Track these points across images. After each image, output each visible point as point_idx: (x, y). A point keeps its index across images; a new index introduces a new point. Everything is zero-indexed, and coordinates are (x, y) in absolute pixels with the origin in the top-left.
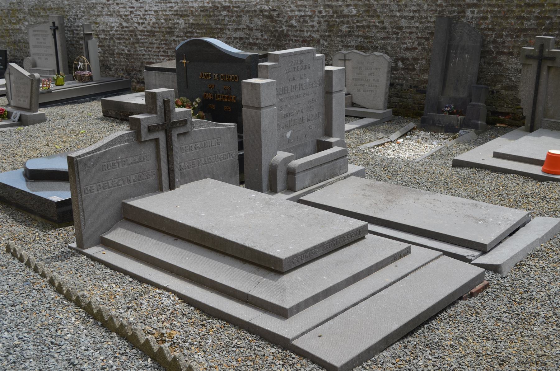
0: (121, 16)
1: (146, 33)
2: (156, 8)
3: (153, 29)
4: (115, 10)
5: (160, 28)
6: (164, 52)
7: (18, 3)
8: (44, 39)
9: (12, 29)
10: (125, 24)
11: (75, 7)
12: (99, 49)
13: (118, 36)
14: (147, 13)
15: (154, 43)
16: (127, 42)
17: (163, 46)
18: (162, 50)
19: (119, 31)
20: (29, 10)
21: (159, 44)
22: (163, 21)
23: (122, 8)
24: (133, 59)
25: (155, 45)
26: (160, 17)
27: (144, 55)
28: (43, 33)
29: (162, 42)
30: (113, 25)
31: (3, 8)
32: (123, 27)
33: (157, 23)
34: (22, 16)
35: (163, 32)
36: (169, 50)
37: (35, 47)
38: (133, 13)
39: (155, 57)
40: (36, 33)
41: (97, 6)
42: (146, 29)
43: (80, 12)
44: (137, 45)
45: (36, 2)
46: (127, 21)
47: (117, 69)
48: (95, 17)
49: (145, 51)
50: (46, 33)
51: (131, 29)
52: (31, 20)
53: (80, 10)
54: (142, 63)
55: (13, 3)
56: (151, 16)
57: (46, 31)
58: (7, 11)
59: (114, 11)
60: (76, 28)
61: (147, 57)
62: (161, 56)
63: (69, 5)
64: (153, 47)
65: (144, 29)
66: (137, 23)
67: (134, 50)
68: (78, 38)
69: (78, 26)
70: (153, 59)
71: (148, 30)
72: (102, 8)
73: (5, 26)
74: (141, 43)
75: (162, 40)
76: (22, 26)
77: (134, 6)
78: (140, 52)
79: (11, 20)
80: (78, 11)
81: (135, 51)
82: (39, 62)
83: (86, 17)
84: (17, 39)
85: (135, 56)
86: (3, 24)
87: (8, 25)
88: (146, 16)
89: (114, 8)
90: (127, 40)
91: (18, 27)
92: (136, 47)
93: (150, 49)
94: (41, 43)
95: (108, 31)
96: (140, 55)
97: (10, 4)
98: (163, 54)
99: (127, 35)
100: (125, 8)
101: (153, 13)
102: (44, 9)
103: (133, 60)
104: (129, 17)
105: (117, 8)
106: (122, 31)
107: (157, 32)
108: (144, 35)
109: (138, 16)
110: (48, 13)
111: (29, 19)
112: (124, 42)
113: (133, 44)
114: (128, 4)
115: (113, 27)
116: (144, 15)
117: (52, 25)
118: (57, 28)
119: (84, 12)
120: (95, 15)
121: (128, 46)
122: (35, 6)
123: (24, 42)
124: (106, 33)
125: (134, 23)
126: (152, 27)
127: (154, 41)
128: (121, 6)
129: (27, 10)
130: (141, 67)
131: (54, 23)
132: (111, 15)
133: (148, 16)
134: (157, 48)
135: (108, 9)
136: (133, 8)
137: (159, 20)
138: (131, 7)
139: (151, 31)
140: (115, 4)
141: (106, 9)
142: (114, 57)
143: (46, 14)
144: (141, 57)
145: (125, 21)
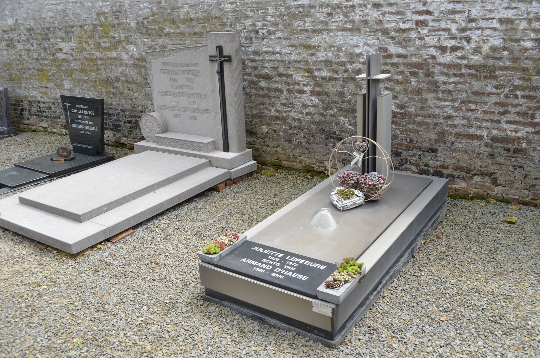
0: (385, 32)
1: (463, 71)
2: (510, 14)
3: (491, 62)
4: (368, 18)
5: (515, 60)
6: (518, 114)
7: (114, 12)
8: (189, 80)
9: (101, 59)
10: (394, 49)
11: (251, 14)
12: (313, 98)
14: (474, 25)
15: (489, 94)
16: (398, 88)
17: (521, 101)
18: (513, 110)
20: (138, 24)
21: (506, 96)
22: (528, 44)
23: (391, 13)
24: (414, 123)
25: (493, 99)
26: (519, 35)
27: (449, 117)
28: (186, 68)
29: (518, 93)
30: (358, 51)
31: (83, 23)
32: (390, 56)
33: (504, 49)
34: (123, 36)
35: (525, 70)
37: (165, 93)
38: (427, 25)
39: (488, 124)
40: (170, 68)
41: (312, 11)
42: (465, 62)
43: (264, 25)
44: (429, 96)
45: (154, 9)
46: (405, 42)
48: (306, 34)
49: (456, 109)
50: (194, 69)
51: (414, 60)
52: (142, 41)
53: (265, 20)
54: (442, 134)
55: (104, 13)
56: (487, 32)
57: (196, 65)
58: (91, 28)
59: (366, 22)
60: (252, 56)
61: (457, 122)
63: (235, 11)
64: (485, 103)
65: (459, 61)
67: (419, 105)
68: (256, 76)
69: (257, 53)
70: (480, 128)
71: (472, 62)
72: (329, 14)
73: (89, 54)
75: (516, 88)
76: (123, 54)
77: (431, 9)
78: (437, 112)
79: (99, 43)
80: (259, 24)
81: (422, 108)
82: (173, 122)
83: (278, 35)
84: (113, 76)
85: (420, 119)
86: (86, 50)
87: (93, 51)
88: (468, 33)
89: (366, 15)
90: (398, 82)
91: (114, 54)
92: (426, 100)
93: (473, 106)
94: (181, 87)
95: (344, 64)
96: (435, 117)
97: (98, 15)
98: (518, 119)
99: (402, 72)
100: (398, 13)
101: (495, 24)
102: (173, 22)
103: (410, 126)
104: (413, 35)
105: (376, 14)
106: (386, 64)
107: (506, 68)
108: (455, 75)
109: (441, 33)
110: (182, 28)
111: (138, 41)
113: (418, 92)
114: (412, 6)
115: (359, 55)
116: (464, 30)
117: (214, 52)
118: (229, 59)
119: (275, 24)
120: (307, 31)
121: (401, 97)
122: (152, 16)
123: (127, 81)
124: (334, 67)
125: (425, 46)
126: (488, 56)
127: (490, 89)
128: (385, 9)
129: (133, 25)
130: (437, 141)
131: (220, 49)
132: (355, 30)
133: (479, 32)
134: (496, 104)
135: (346, 16)
136: (428, 13)
137: (517, 41)
138: (421, 13)
139: (485, 66)
140: (369, 6)
141: (342, 17)
143: (177, 31)
144: (441, 120)
145: (399, 43)
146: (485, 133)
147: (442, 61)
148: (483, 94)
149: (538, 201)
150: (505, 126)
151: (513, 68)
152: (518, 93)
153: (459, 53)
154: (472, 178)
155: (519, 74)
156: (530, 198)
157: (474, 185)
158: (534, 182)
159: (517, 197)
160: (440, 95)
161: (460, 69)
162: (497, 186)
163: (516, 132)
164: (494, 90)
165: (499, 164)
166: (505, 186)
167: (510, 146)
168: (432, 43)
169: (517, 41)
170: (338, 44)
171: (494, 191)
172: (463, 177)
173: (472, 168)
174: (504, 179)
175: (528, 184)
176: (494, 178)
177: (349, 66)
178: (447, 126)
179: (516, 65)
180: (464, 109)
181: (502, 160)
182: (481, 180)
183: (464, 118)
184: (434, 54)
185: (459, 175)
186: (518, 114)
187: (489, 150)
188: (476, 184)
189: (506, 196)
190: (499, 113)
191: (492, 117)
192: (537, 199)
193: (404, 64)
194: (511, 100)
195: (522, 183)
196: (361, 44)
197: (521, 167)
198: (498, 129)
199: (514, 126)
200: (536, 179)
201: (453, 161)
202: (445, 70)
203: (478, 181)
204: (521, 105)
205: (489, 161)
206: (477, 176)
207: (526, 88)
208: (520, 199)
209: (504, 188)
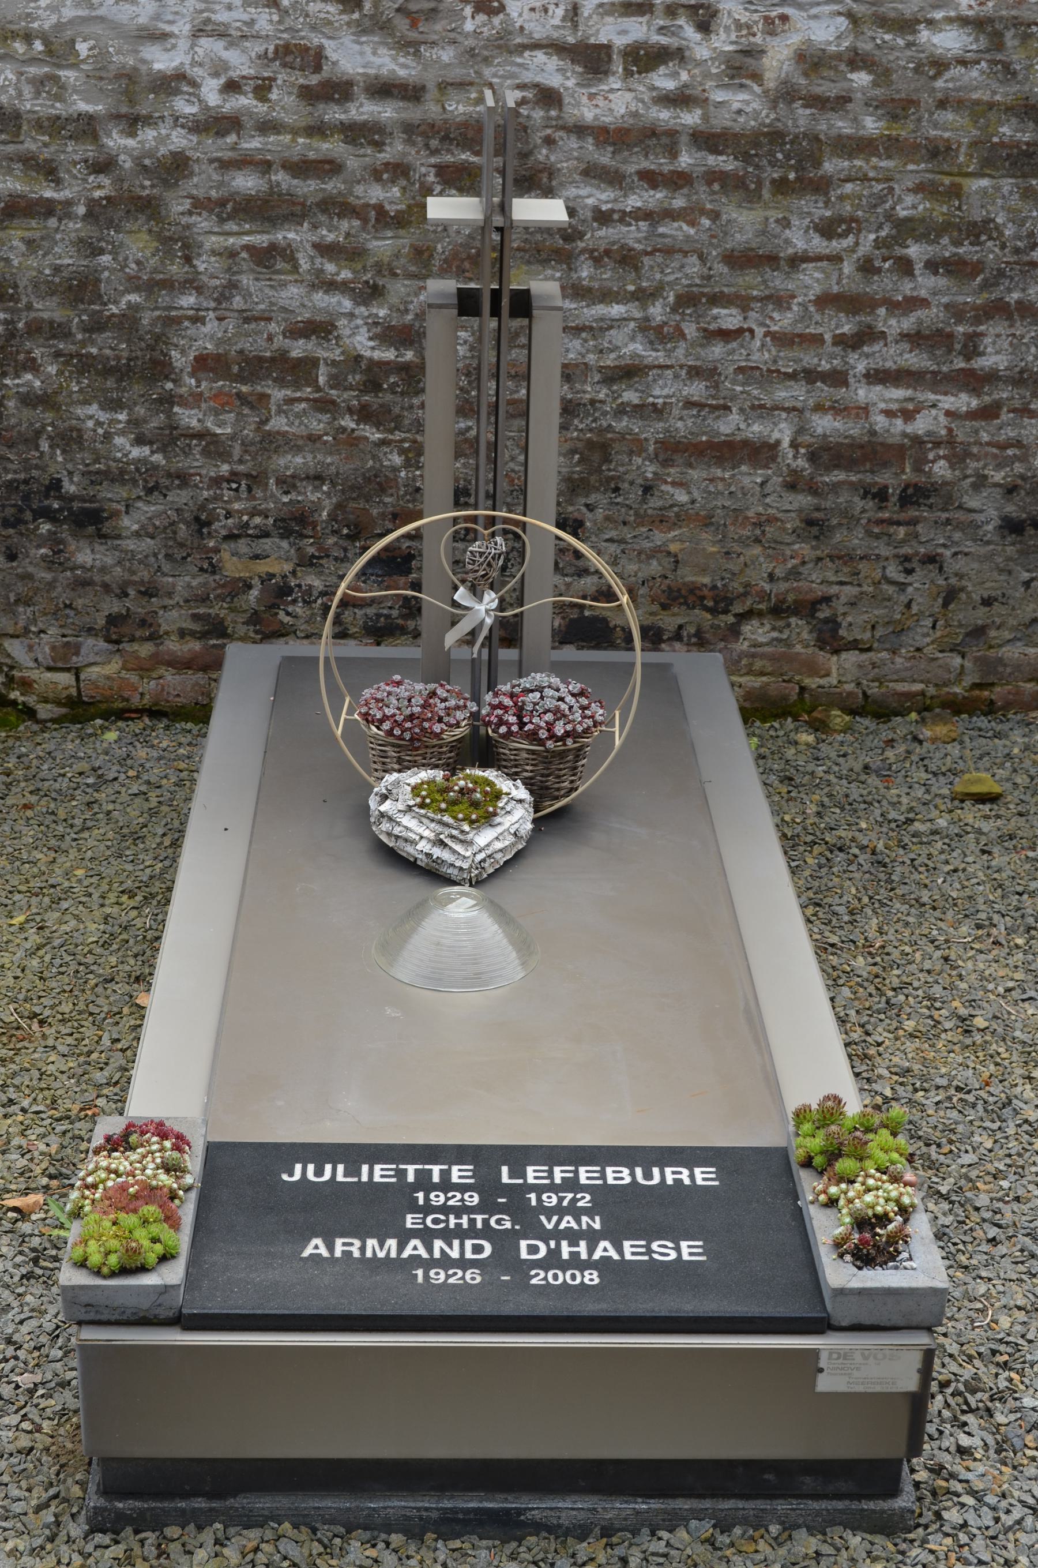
1: (686, 160)
3: (802, 117)
6: (915, 339)
13: (246, 182)
15: (797, 261)
17: (925, 283)
18: (894, 325)
19: (267, 127)
21: (867, 267)
29: (914, 251)
33: (856, 60)
36: (993, 331)
39: (795, 393)
42: (691, 118)
47: (201, 524)
51: (458, 108)
61: (662, 390)
62: (878, 377)
64: (780, 301)
65: (664, 115)
66: (556, 48)
70: (762, 410)
71: (722, 121)
74: (597, 259)
93: (729, 318)
98: (914, 360)
99: (399, 170)
106: (318, 130)
107: (863, 146)
108: (650, 179)
112: (325, 250)
124: (32, 143)
134: (824, 301)
137: (906, 25)
139: (776, 136)
142: (168, 401)
146: (783, 432)
147: (588, 115)
148: (772, 260)
149: (998, 689)
150: (863, 393)
151: (891, 146)
152: (914, 251)
153: (663, 80)
154: (734, 632)
155: (917, 169)
156: (968, 681)
157: (744, 662)
158: (979, 616)
159: (918, 687)
160: (585, 272)
161: (674, 154)
162: (836, 652)
163: (908, 416)
164: (818, 244)
165: (844, 557)
166: (869, 649)
167: (885, 478)
168: (538, 30)
169: (906, 25)
170: (47, 22)
171: (828, 675)
172: (699, 633)
173: (736, 586)
174: (865, 617)
175: (960, 626)
176: (826, 621)
177: (116, 141)
178: (621, 411)
179: (903, 132)
180: (690, 330)
181: (856, 540)
182: (775, 634)
183: (695, 373)
184: (554, 81)
185: (680, 627)
186: (915, 339)
187: (803, 500)
188: (753, 656)
189: (874, 690)
190: (840, 340)
191: (809, 360)
192: (993, 684)
193: (409, 129)
194: (885, 284)
195: (934, 627)
196: (182, 28)
197: (931, 559)
198: (838, 409)
199: (899, 393)
200: (987, 602)
201: (654, 567)
202: (605, 158)
203: (762, 639)
204: (924, 303)
205: (804, 549)
206: (755, 622)
207: (946, 227)
208: (932, 691)
209: (865, 656)
